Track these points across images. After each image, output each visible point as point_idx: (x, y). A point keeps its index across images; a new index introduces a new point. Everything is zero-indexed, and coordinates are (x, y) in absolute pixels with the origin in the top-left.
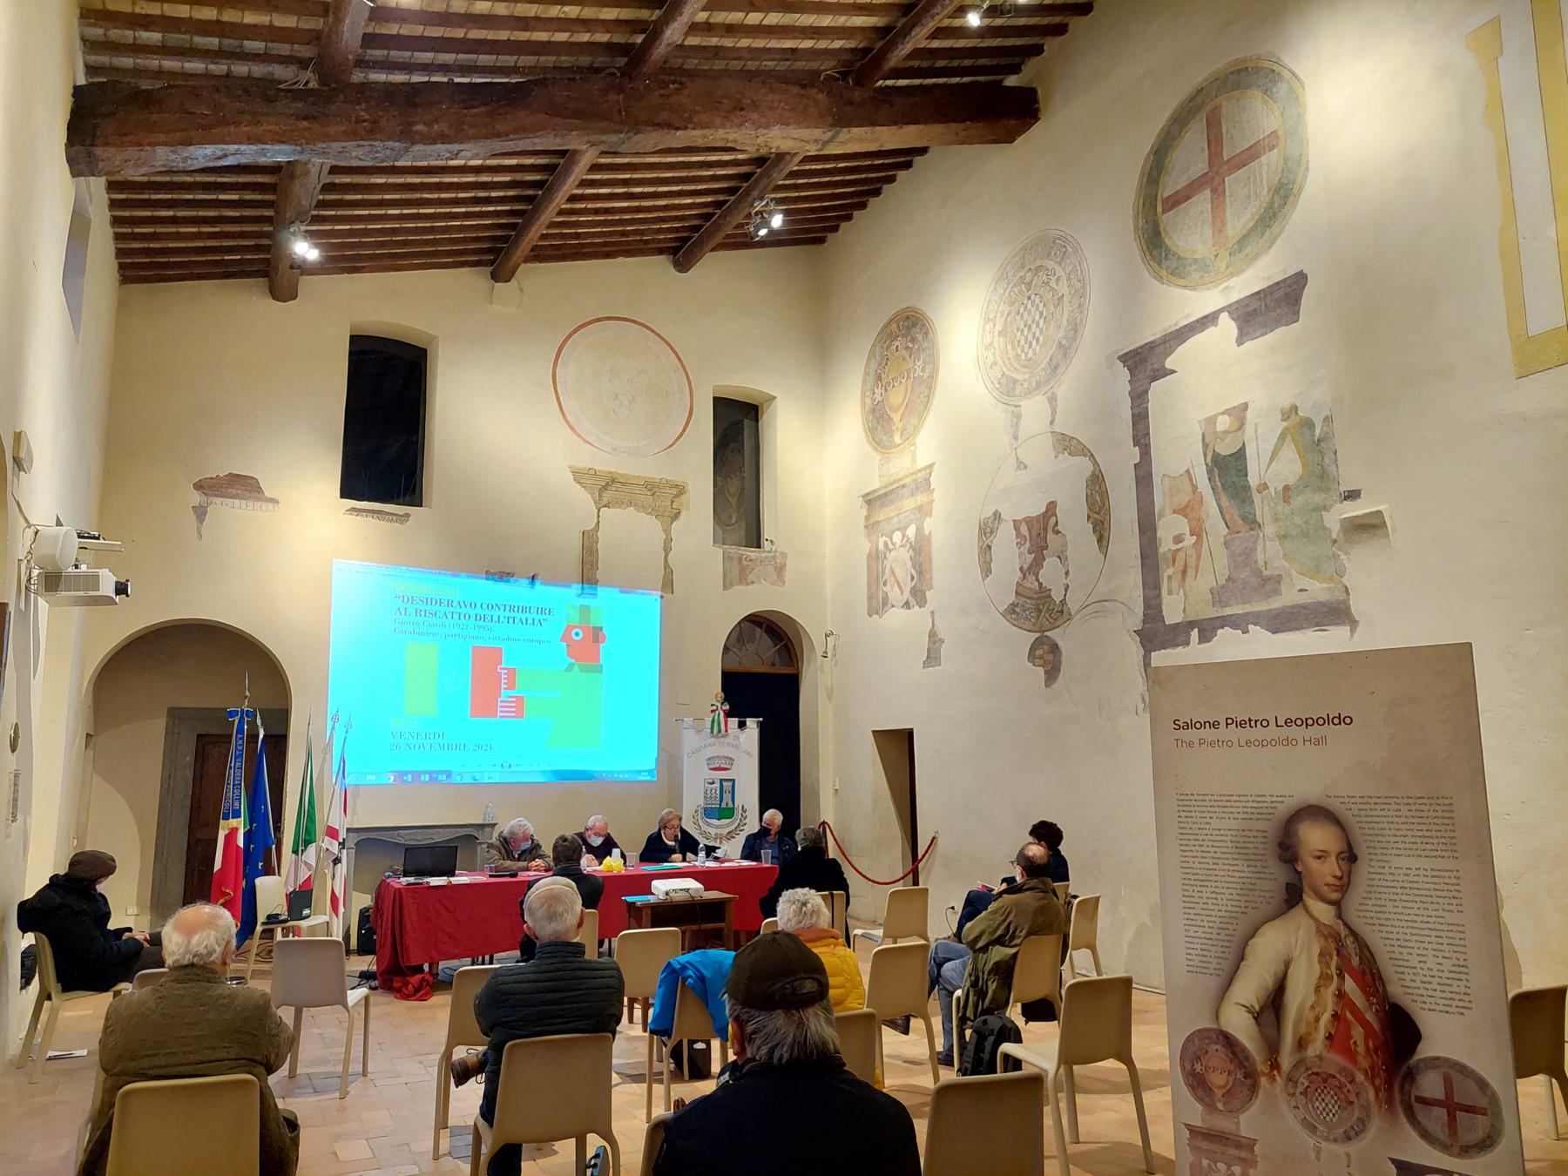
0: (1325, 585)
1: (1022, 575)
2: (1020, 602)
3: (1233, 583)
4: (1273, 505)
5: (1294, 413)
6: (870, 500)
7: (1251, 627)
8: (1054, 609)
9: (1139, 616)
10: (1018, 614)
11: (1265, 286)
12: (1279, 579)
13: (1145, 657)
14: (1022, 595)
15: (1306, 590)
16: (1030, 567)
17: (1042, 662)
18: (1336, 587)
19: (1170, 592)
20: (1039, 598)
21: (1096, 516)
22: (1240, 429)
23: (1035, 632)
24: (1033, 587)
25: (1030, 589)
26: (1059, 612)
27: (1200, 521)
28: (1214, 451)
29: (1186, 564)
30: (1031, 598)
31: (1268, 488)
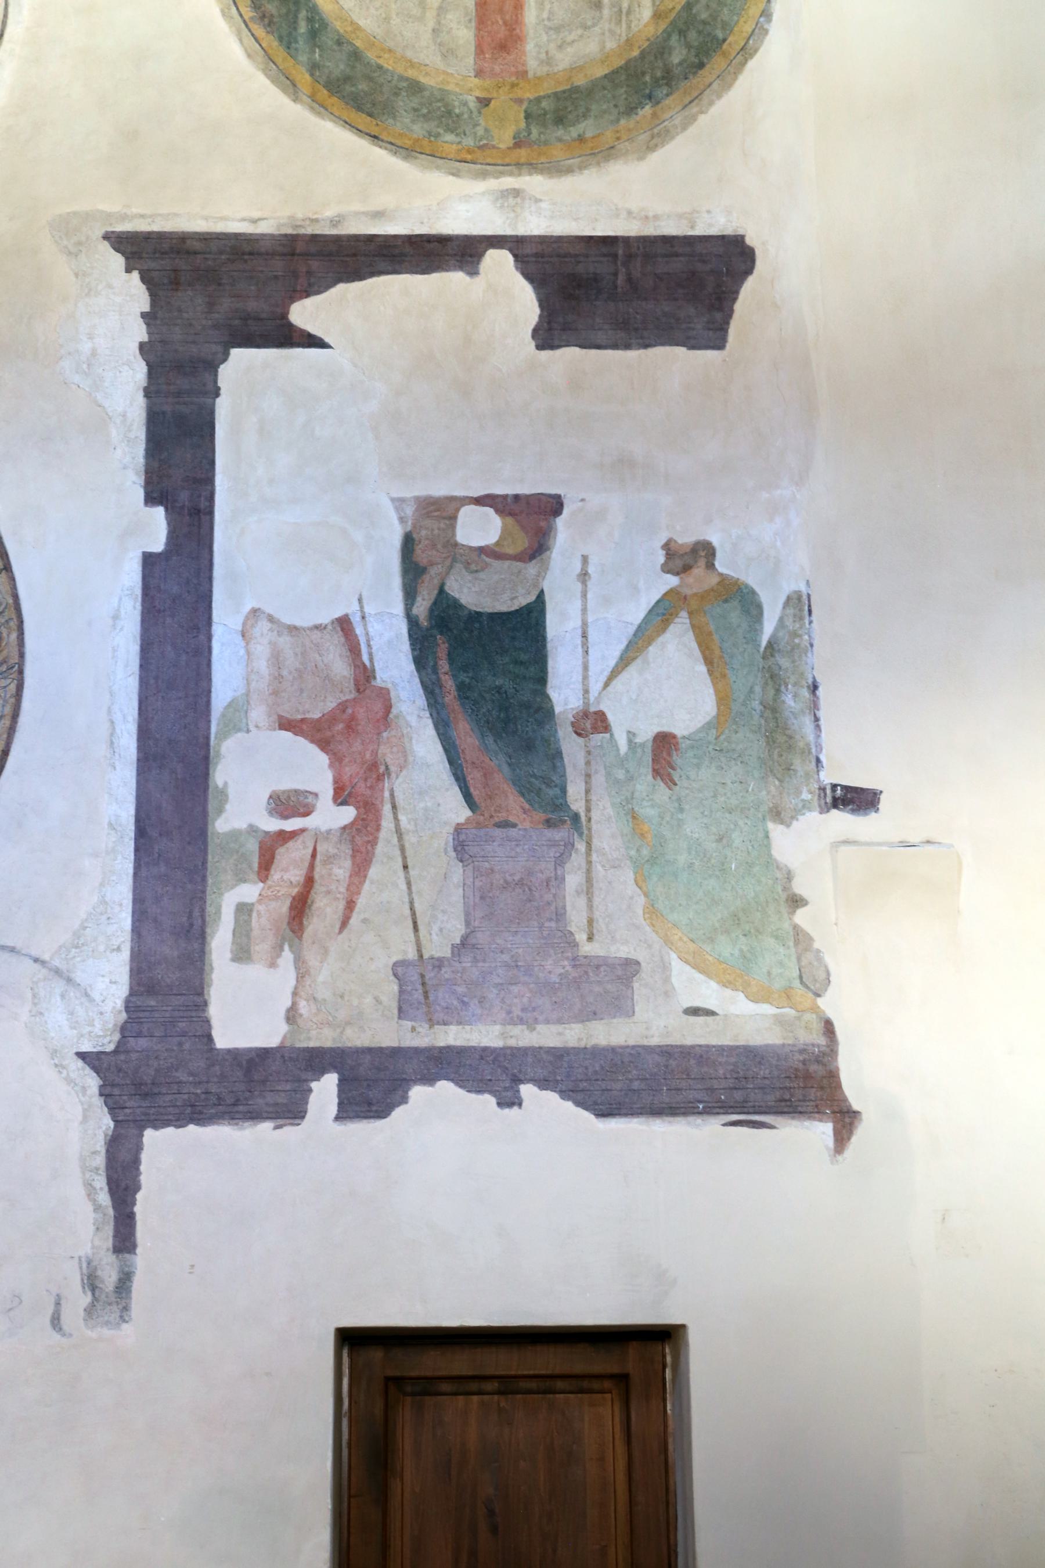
0: (767, 1009)
3: (475, 960)
4: (620, 774)
5: (702, 562)
7: (527, 1090)
9: (108, 1007)
11: (633, 234)
12: (629, 968)
13: (114, 1143)
18: (798, 1018)
19: (242, 954)
22: (532, 557)
28: (441, 591)
29: (309, 881)
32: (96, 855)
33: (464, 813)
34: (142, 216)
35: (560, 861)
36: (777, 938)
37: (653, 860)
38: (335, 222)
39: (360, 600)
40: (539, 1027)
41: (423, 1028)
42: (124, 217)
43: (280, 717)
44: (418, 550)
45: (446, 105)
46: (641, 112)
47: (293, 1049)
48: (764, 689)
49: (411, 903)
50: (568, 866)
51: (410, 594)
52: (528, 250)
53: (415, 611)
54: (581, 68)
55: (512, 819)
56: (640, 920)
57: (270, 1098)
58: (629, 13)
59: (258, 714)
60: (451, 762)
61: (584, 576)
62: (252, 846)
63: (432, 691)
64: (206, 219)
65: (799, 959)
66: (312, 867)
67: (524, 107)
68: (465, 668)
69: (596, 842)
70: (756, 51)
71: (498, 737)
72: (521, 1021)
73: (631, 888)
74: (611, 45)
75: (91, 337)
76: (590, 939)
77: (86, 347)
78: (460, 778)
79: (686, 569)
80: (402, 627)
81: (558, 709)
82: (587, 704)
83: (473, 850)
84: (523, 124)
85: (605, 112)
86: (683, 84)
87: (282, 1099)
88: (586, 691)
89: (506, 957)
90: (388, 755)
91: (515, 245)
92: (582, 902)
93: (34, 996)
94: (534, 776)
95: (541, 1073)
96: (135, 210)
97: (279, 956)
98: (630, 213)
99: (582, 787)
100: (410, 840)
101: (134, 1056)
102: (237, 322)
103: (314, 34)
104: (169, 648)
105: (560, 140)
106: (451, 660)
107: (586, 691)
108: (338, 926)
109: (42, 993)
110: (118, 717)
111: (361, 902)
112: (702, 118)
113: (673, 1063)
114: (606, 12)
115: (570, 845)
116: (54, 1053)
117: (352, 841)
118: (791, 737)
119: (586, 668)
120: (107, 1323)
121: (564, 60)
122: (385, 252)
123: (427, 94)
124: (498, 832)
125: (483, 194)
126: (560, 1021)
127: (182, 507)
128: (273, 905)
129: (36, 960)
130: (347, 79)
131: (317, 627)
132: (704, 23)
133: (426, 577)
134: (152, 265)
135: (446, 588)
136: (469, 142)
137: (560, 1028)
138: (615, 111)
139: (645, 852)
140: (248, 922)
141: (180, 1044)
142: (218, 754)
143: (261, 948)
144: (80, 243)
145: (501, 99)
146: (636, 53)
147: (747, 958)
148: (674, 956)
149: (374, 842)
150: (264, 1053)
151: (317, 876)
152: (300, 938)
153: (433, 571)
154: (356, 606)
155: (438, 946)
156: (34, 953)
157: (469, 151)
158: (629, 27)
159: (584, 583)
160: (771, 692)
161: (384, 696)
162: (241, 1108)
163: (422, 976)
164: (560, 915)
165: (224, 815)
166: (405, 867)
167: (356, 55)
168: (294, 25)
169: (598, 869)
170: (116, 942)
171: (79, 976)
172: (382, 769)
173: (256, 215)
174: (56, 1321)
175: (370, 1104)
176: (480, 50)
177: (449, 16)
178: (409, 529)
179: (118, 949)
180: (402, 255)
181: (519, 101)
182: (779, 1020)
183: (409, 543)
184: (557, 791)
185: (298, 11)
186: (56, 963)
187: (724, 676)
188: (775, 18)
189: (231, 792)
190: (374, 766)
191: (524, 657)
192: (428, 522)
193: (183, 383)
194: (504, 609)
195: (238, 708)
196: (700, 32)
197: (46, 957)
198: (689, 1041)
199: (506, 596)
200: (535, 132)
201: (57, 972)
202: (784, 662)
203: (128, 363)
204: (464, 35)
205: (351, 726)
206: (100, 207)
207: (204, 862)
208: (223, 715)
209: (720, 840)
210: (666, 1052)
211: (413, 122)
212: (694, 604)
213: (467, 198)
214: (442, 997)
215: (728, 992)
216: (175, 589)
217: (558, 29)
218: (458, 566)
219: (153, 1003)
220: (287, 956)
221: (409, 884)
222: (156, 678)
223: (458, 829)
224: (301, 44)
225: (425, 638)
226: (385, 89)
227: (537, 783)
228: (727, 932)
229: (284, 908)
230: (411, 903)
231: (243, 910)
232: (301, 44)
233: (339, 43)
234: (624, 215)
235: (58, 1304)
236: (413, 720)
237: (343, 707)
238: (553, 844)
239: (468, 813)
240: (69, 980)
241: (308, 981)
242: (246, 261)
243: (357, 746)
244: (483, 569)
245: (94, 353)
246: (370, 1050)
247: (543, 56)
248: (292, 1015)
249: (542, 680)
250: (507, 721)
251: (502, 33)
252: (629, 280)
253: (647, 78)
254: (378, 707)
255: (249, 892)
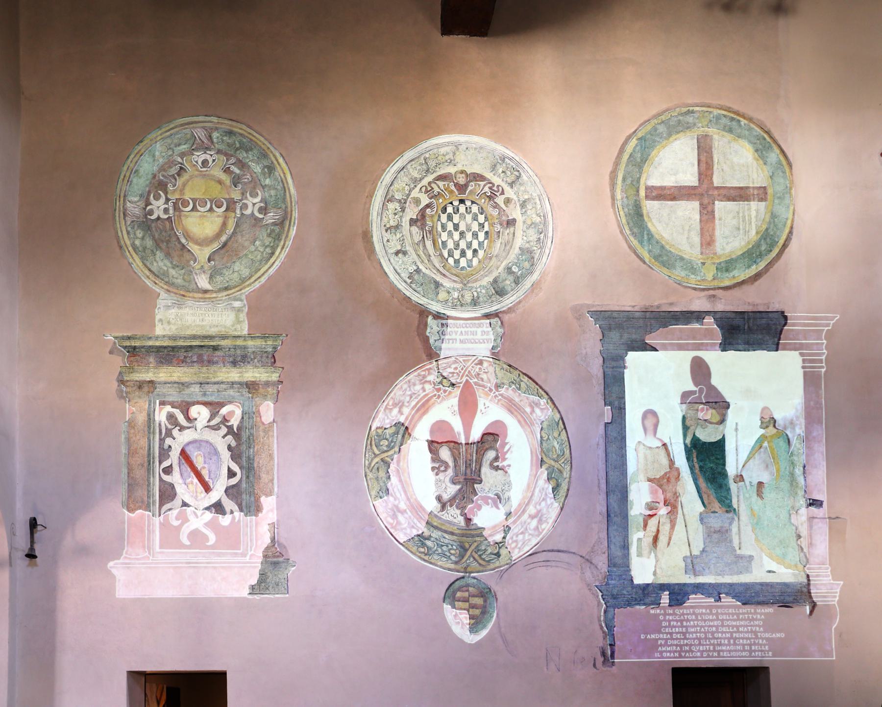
0: (790, 571)
1: (439, 506)
2: (433, 535)
5: (772, 425)
6: (135, 348)
8: (485, 550)
10: (429, 548)
12: (751, 558)
14: (436, 528)
15: (774, 572)
16: (452, 500)
17: (466, 605)
19: (639, 555)
20: (463, 535)
21: (553, 463)
22: (721, 423)
23: (458, 571)
24: (455, 521)
25: (450, 523)
26: (495, 554)
27: (676, 495)
28: (694, 435)
29: (658, 531)
30: (452, 534)
31: (743, 480)
32: (596, 523)
33: (702, 509)
34: (599, 305)
35: (731, 524)
36: (793, 548)
37: (757, 524)
38: (658, 307)
39: (670, 438)
40: (725, 576)
41: (692, 577)
42: (593, 306)
43: (648, 477)
44: (687, 422)
45: (691, 265)
46: (752, 267)
47: (655, 584)
48: (789, 467)
49: (688, 538)
50: (733, 525)
51: (685, 436)
52: (718, 316)
53: (686, 442)
54: (733, 252)
55: (716, 510)
56: (753, 542)
57: (650, 599)
58: (748, 232)
59: (642, 477)
60: (698, 492)
61: (736, 429)
62: (641, 520)
63: (692, 468)
64: (618, 306)
65: (799, 555)
66: (658, 526)
67: (716, 266)
68: (701, 461)
69: (741, 518)
70: (788, 245)
71: (711, 484)
72: (720, 575)
73: (751, 533)
74: (743, 243)
75: (585, 349)
76: (740, 549)
77: (584, 352)
78: (701, 497)
79: (767, 427)
80: (683, 447)
81: (729, 474)
82: (737, 472)
83: (705, 520)
84: (716, 272)
85: (741, 267)
86: (766, 257)
87: (653, 599)
88: (737, 468)
89: (715, 555)
90: (679, 490)
91: (713, 313)
92: (737, 537)
93: (582, 568)
94: (722, 496)
95: (726, 590)
96: (596, 303)
97: (650, 555)
98: (749, 303)
99: (736, 500)
100: (687, 517)
101: (611, 586)
102: (629, 342)
103: (649, 239)
104: (614, 455)
105: (727, 277)
106: (697, 458)
107: (737, 468)
108: (667, 545)
109: (583, 566)
110: (600, 478)
111: (673, 538)
112: (771, 270)
113: (763, 588)
114: (741, 231)
115: (733, 519)
116: (588, 585)
117: (670, 518)
118: (797, 483)
119: (737, 460)
120: (609, 666)
121: (728, 249)
122: (674, 317)
123: (685, 261)
124: (712, 515)
125: (704, 296)
126: (731, 575)
127: (616, 407)
128: (648, 539)
129: (581, 556)
130: (660, 256)
131: (657, 447)
132: (772, 235)
133: (689, 430)
134: (603, 323)
135: (696, 434)
136: (699, 278)
137: (731, 577)
138: (744, 267)
139: (755, 521)
140: (641, 544)
141: (624, 583)
142: (630, 490)
143: (645, 552)
144: (580, 315)
145: (709, 262)
146: (751, 246)
147: (784, 555)
148: (763, 554)
149: (676, 518)
150: (648, 585)
151: (660, 529)
152: (656, 549)
153: (692, 428)
154: (669, 440)
155: (696, 552)
156: (581, 554)
157: (699, 281)
158: (748, 237)
159: (736, 431)
160: (792, 468)
161: (678, 469)
162: (642, 602)
163: (692, 561)
164: (731, 541)
165: (633, 510)
166: (686, 526)
167: (663, 247)
168: (643, 236)
169: (742, 527)
170: (603, 551)
171: (594, 561)
172: (678, 494)
173: (634, 304)
174: (594, 665)
175: (678, 601)
176: (702, 245)
177: (692, 233)
178: (684, 414)
179: (604, 553)
180: (679, 318)
181: (714, 263)
182: (794, 574)
183: (684, 418)
184: (729, 501)
185: (644, 231)
186: (587, 557)
187: (778, 463)
188: (794, 234)
189: (634, 502)
190: (675, 493)
191: (718, 457)
192: (690, 412)
193: (614, 364)
194: (713, 441)
195: (636, 474)
196: (770, 239)
197: (584, 555)
198: (768, 581)
199: (713, 437)
200: (719, 274)
201: (587, 560)
202: (795, 458)
203: (597, 357)
204: (697, 239)
205: (668, 480)
206: (586, 302)
207: (628, 525)
208: (631, 477)
209: (776, 517)
210: (762, 584)
211: (681, 271)
212: (769, 439)
213: (699, 298)
214: (697, 568)
215: (779, 566)
216: (615, 435)
217: (726, 238)
218: (699, 427)
219: (615, 569)
220: (653, 554)
221: (687, 531)
222: (611, 465)
223: (701, 514)
224: (645, 243)
225: (689, 451)
226: (672, 259)
227: (723, 498)
228: (778, 546)
229: (651, 539)
230: (688, 538)
231: (639, 540)
232: (645, 243)
233: (657, 242)
234: (747, 304)
235: (595, 660)
236: (686, 478)
237: (666, 474)
238: (728, 518)
239: (704, 509)
240: (591, 563)
241: (659, 562)
242: (631, 321)
243: (671, 487)
244: (706, 428)
245: (586, 354)
246: (677, 584)
247: (721, 247)
248: (655, 574)
249: (724, 465)
250: (714, 478)
251: (709, 239)
252: (749, 327)
253: (754, 255)
254: (676, 474)
255: (641, 534)
